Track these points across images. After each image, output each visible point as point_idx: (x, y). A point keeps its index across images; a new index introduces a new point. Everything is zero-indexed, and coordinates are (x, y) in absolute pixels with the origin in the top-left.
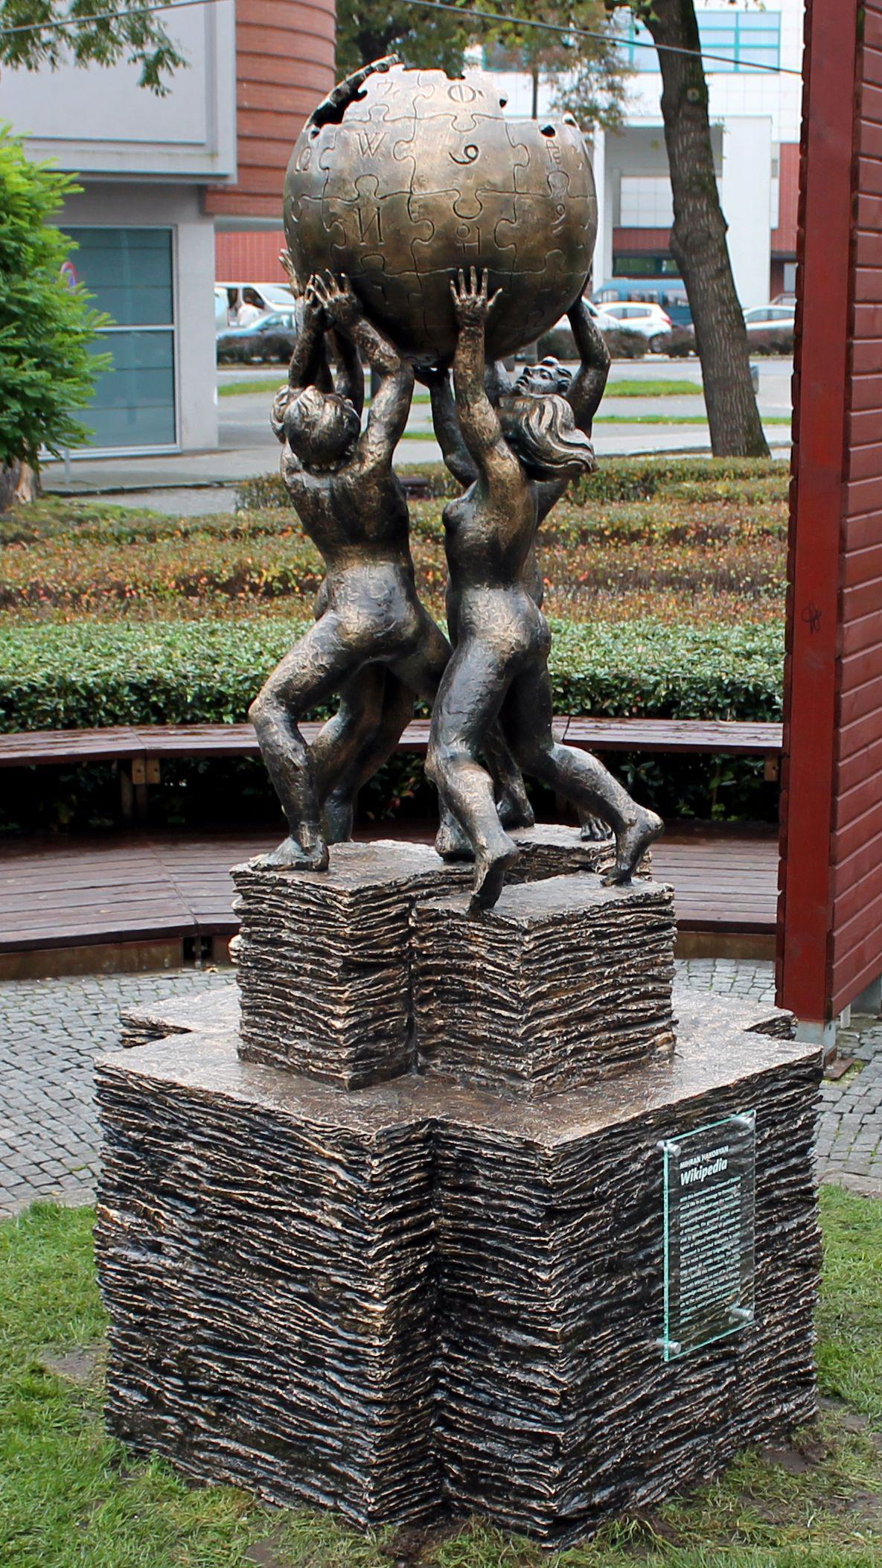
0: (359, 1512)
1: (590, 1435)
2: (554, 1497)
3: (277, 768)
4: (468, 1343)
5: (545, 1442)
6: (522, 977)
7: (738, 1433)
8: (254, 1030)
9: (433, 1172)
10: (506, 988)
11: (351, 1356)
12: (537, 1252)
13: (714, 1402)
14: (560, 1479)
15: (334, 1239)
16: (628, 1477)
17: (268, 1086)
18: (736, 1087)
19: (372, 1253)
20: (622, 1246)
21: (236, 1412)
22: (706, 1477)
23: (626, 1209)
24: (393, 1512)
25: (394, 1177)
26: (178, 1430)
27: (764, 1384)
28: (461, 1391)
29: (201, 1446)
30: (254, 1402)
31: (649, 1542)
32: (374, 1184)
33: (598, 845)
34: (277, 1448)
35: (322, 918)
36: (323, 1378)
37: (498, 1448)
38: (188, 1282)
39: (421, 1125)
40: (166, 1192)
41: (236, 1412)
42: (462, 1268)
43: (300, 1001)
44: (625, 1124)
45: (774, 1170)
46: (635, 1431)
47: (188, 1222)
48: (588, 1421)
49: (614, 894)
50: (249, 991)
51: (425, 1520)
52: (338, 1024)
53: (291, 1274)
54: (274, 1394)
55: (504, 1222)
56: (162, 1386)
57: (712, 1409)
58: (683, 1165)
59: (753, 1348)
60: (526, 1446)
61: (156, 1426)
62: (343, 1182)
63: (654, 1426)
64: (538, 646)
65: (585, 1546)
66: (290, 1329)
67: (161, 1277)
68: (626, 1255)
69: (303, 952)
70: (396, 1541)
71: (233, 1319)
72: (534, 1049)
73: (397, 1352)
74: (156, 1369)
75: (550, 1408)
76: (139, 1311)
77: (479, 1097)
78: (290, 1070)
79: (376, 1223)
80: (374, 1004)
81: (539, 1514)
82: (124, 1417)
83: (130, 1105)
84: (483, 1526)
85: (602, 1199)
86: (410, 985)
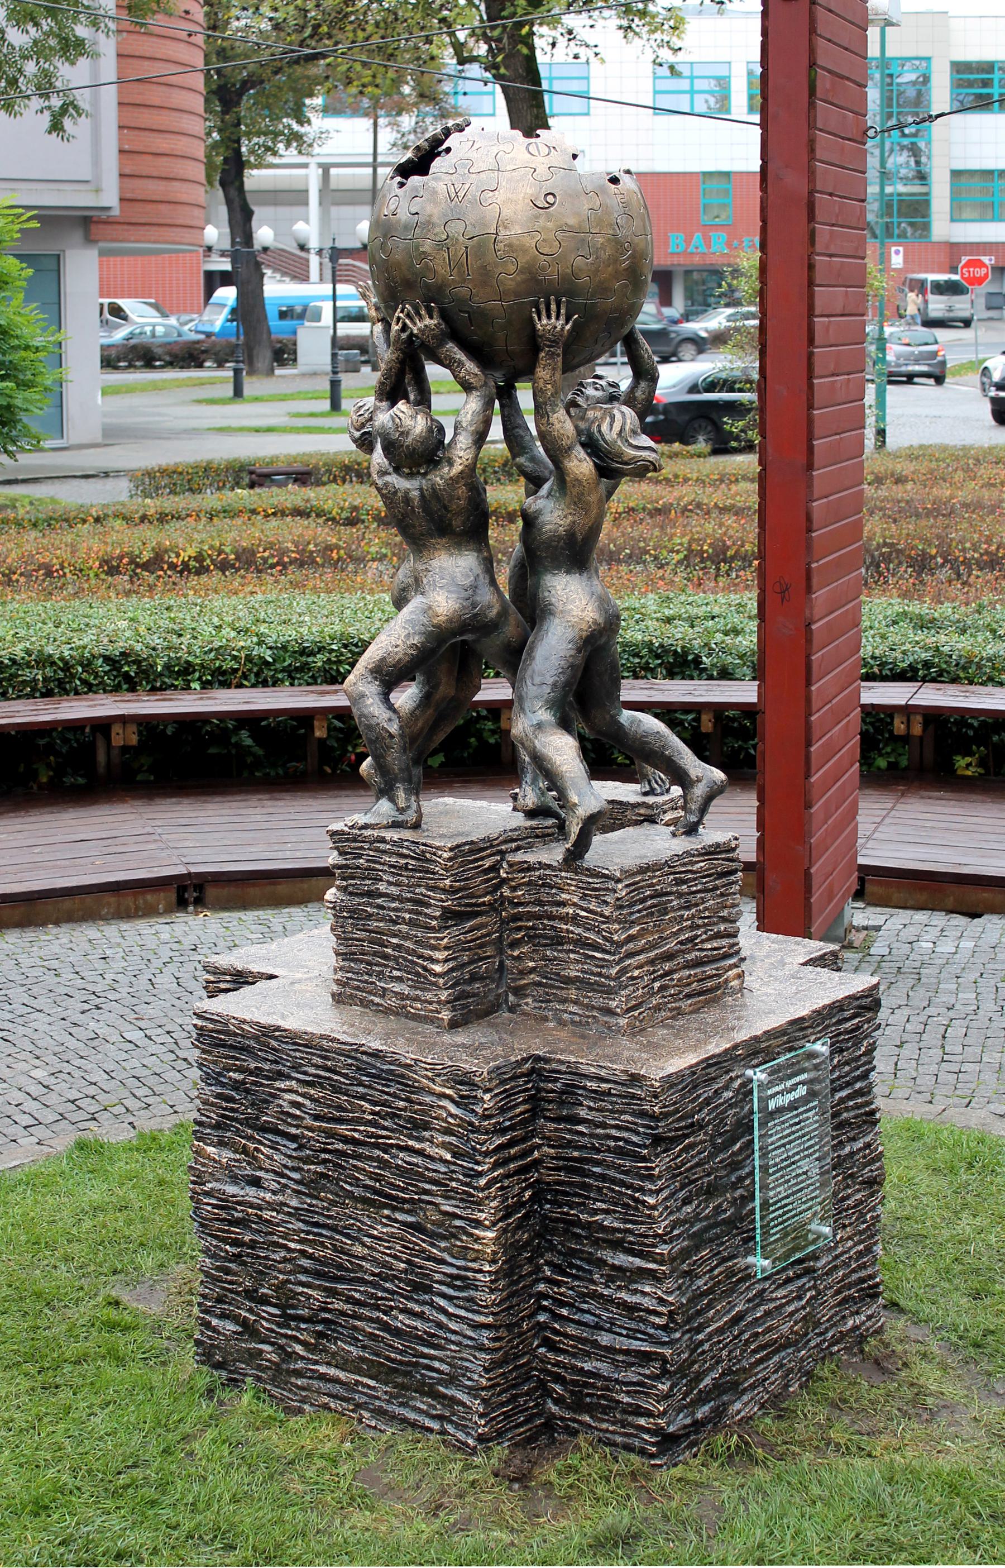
0: (468, 1434)
1: (693, 1351)
2: (662, 1414)
3: (373, 736)
4: (571, 1266)
5: (652, 1360)
6: (615, 921)
7: (817, 1345)
8: (349, 975)
9: (536, 1102)
10: (598, 932)
11: (461, 1281)
12: (643, 1178)
13: (798, 1316)
14: (666, 1397)
15: (443, 1169)
16: (725, 1392)
17: (370, 1026)
18: (810, 1017)
19: (483, 1182)
20: (717, 1170)
21: (336, 1338)
22: (791, 1389)
23: (721, 1134)
24: (500, 1434)
25: (503, 1110)
26: (274, 1358)
27: (840, 1297)
28: (565, 1312)
29: (298, 1373)
30: (355, 1328)
31: (750, 1455)
32: (486, 1117)
33: (660, 799)
34: (380, 1373)
35: (420, 872)
36: (431, 1304)
37: (604, 1367)
38: (289, 1214)
39: (525, 1060)
40: (264, 1129)
41: (336, 1338)
42: (566, 1194)
43: (398, 947)
44: (719, 1055)
45: (843, 1094)
46: (731, 1347)
47: (290, 1157)
48: (691, 1338)
49: (681, 845)
50: (343, 939)
51: (529, 1440)
52: (438, 968)
53: (396, 1204)
54: (378, 1320)
55: (609, 1150)
56: (258, 1315)
57: (796, 1323)
58: (770, 1092)
59: (829, 1263)
60: (633, 1364)
61: (251, 1355)
62: (452, 1115)
63: (747, 1340)
64: (611, 623)
65: (691, 1462)
66: (395, 1257)
67: (261, 1209)
68: (721, 1178)
69: (401, 902)
70: (507, 1463)
71: (335, 1248)
72: (626, 987)
73: (506, 1276)
74: (252, 1299)
75: (658, 1327)
76: (236, 1243)
77: (574, 1033)
78: (387, 1011)
79: (487, 1154)
80: (470, 949)
81: (648, 1431)
82: (217, 1347)
83: (232, 1047)
84: (590, 1444)
85: (701, 1126)
86: (500, 930)
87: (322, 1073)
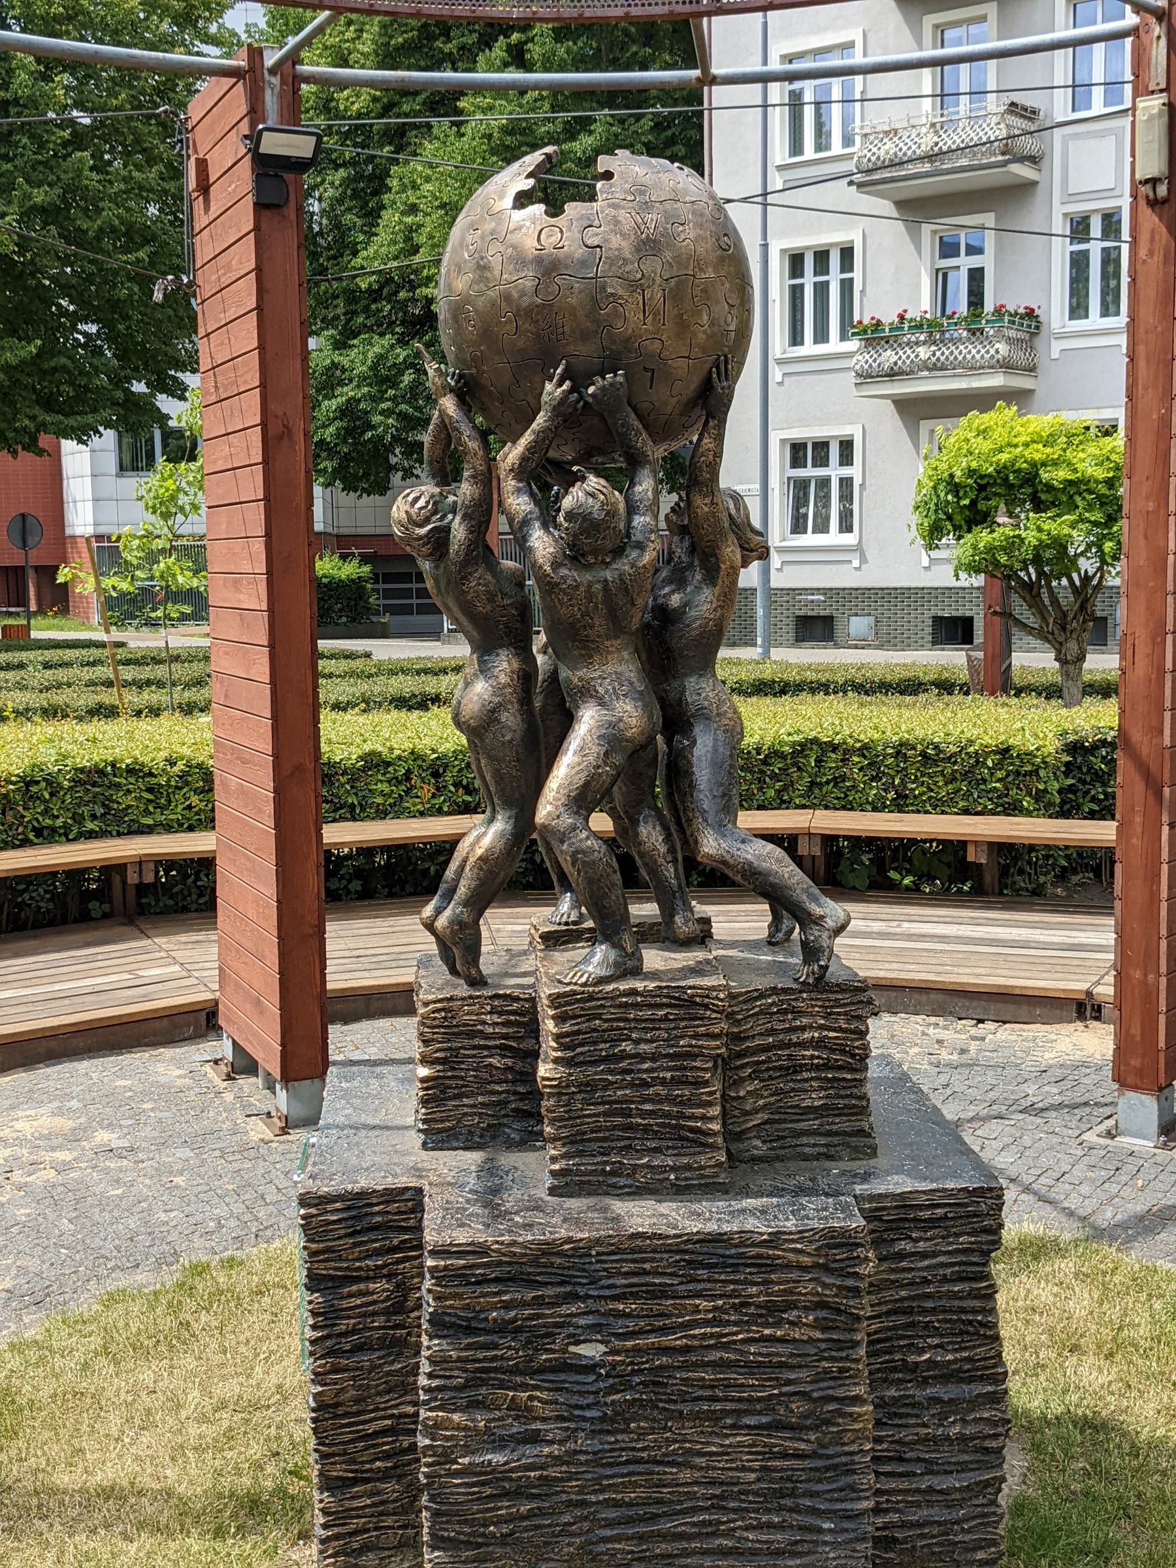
66: (744, 1469)
87: (635, 1280)
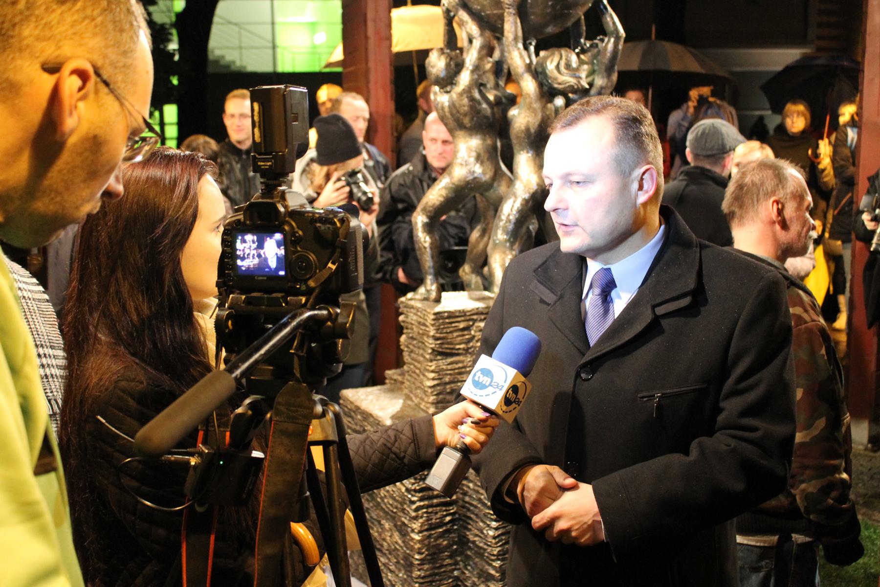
19: (414, 507)
80: (450, 374)
